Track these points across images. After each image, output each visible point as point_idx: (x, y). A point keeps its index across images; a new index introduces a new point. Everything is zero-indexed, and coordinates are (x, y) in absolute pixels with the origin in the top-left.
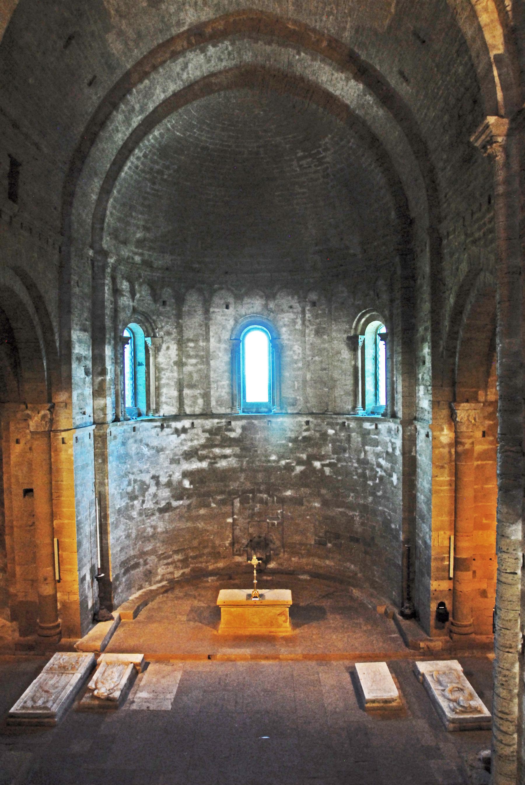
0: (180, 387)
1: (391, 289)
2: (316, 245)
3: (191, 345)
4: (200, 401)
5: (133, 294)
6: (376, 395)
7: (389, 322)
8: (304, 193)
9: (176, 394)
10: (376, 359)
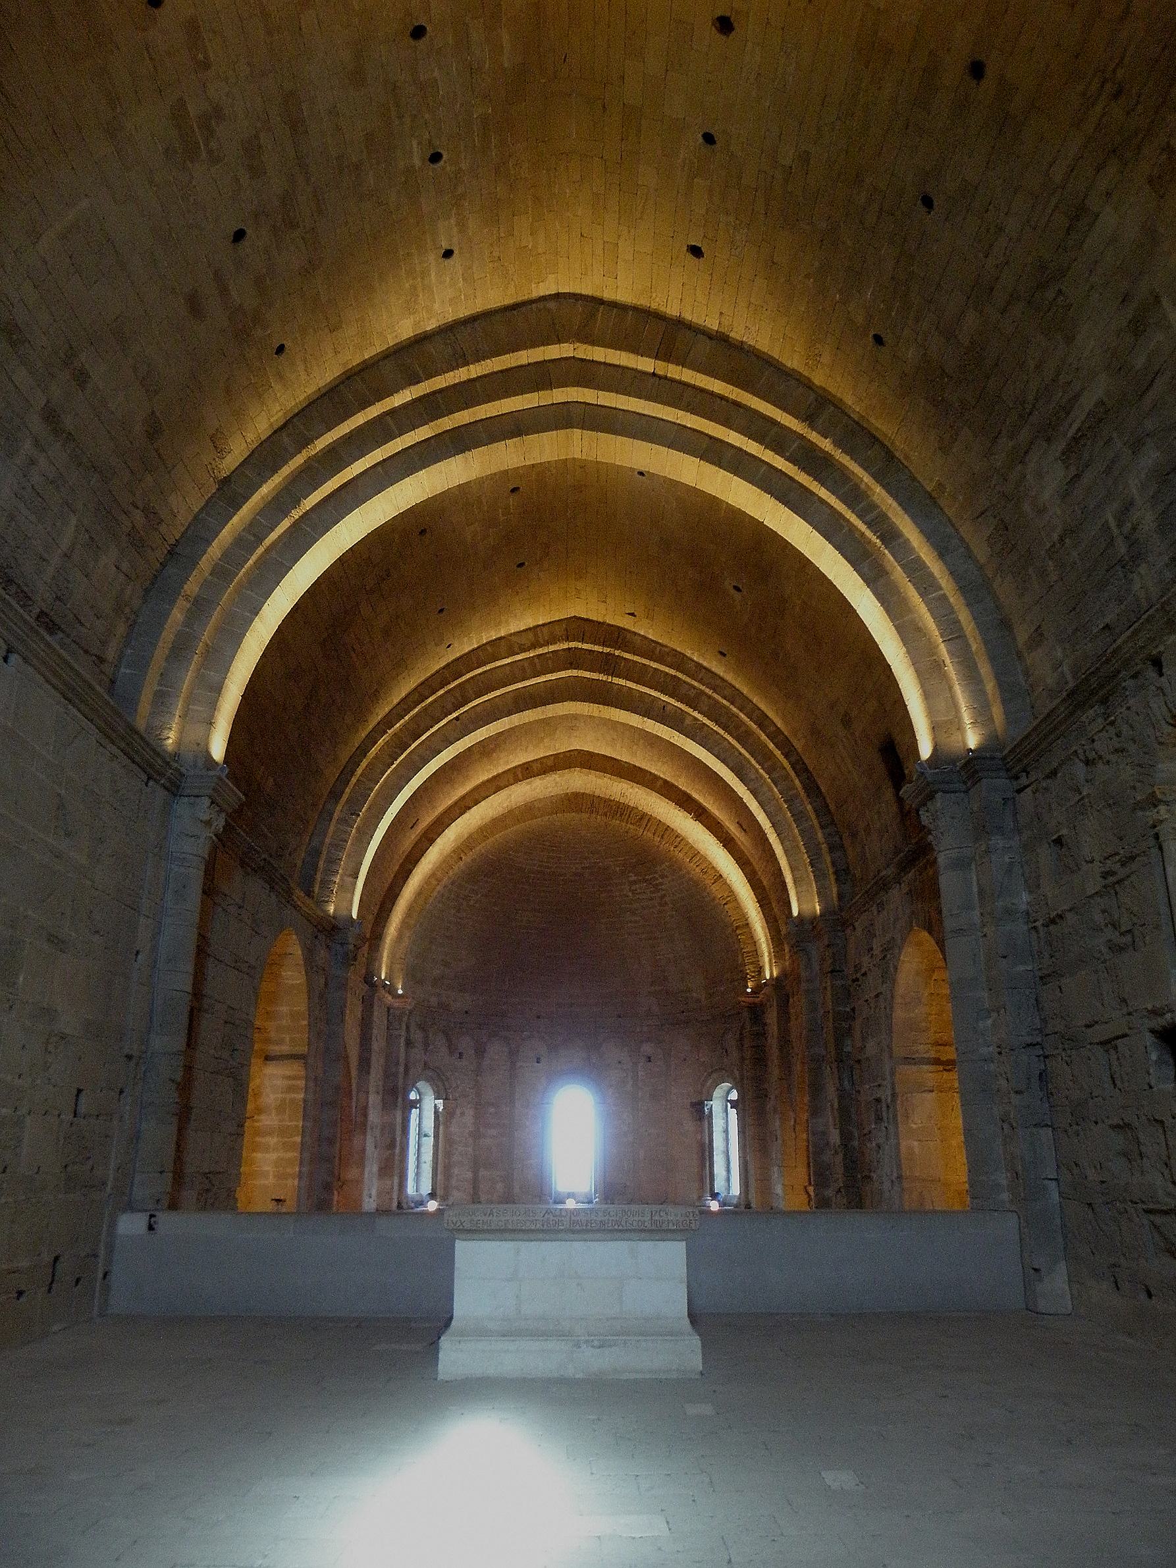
0: (476, 1165)
1: (741, 1047)
2: (652, 984)
3: (492, 1110)
4: (500, 1186)
5: (426, 1044)
6: (728, 1180)
7: (739, 1085)
8: (636, 922)
9: (469, 1175)
10: (726, 1131)
